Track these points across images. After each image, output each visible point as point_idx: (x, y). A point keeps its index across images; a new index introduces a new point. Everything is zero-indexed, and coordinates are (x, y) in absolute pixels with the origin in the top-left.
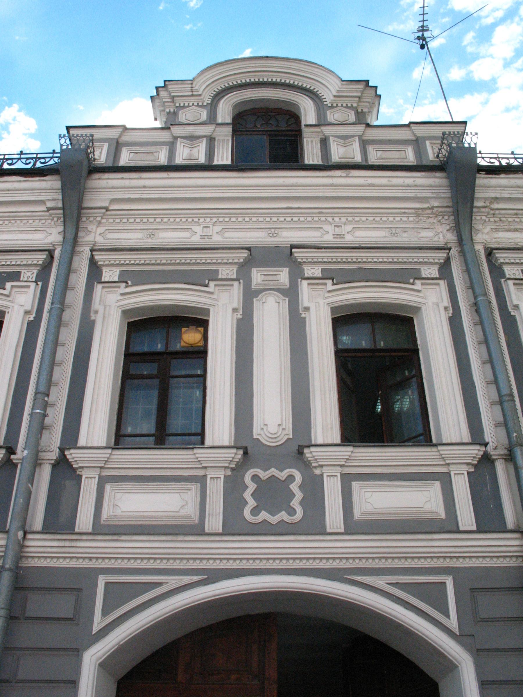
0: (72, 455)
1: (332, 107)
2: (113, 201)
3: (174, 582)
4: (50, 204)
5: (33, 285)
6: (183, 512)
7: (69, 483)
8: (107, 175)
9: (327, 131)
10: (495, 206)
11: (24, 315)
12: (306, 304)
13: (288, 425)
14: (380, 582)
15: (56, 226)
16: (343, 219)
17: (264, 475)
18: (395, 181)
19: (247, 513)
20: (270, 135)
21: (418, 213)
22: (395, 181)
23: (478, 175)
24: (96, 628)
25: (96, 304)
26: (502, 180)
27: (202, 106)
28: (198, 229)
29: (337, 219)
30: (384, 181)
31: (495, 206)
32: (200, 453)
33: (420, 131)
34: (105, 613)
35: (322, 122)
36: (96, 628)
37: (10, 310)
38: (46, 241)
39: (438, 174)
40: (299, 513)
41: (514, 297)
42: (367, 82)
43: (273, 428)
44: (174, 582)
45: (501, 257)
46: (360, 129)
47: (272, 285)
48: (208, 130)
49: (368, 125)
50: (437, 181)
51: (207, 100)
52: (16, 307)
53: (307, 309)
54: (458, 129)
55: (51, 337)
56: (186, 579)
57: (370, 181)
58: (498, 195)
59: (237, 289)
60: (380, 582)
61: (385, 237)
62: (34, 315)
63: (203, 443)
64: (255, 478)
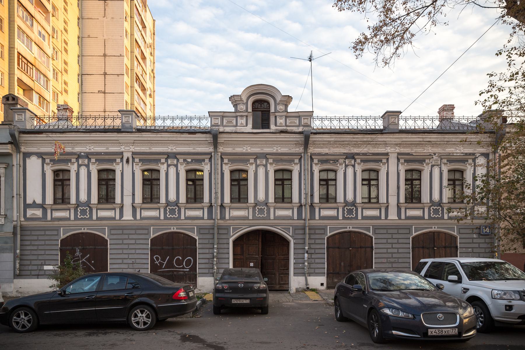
0: (224, 205)
1: (279, 104)
2: (225, 141)
3: (244, 227)
4: (209, 141)
6: (245, 215)
7: (223, 209)
8: (222, 134)
9: (277, 114)
10: (314, 142)
12: (269, 170)
13: (264, 198)
14: (279, 227)
15: (211, 146)
16: (278, 146)
17: (260, 208)
18: (291, 136)
19: (256, 215)
20: (262, 112)
21: (296, 144)
22: (291, 136)
23: (311, 135)
24: (231, 235)
25: (224, 169)
26: (317, 136)
27: (244, 104)
28: (244, 148)
29: (277, 146)
30: (288, 136)
31: (314, 142)
32: (248, 204)
33: (300, 114)
34: (232, 233)
35: (276, 111)
36: (231, 235)
38: (209, 151)
39: (302, 135)
40: (266, 215)
41: (314, 168)
42: (289, 96)
43: (261, 199)
44: (244, 227)
45: (313, 157)
46: (285, 114)
47: (261, 164)
48: (246, 114)
49: (288, 112)
50: (301, 136)
51: (245, 101)
52: (206, 169)
53: (269, 171)
54: (310, 114)
56: (246, 227)
57: (285, 136)
58: (316, 140)
59: (254, 165)
60: (279, 227)
61: (288, 150)
63: (248, 202)
64: (258, 208)
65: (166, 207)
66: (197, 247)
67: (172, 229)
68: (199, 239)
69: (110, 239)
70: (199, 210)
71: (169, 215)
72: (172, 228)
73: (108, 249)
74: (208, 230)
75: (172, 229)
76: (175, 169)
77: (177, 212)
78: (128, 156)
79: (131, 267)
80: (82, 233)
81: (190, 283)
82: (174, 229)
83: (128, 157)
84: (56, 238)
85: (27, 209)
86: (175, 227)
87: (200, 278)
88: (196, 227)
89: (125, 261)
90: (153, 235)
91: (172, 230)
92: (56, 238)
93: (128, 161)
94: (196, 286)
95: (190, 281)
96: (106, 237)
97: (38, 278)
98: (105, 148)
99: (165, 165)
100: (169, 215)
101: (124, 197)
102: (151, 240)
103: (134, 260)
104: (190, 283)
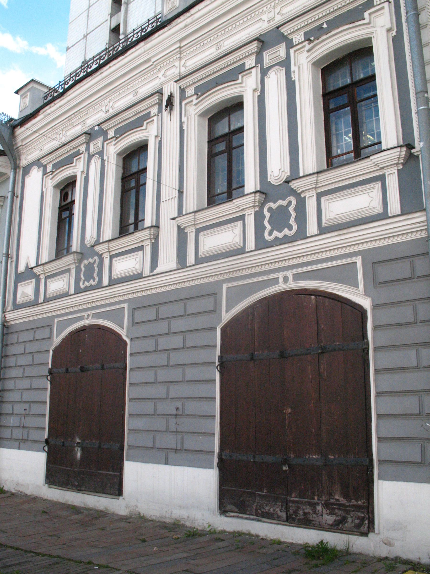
5: (386, 5)
11: (387, 34)
37: (374, 34)
52: (379, 29)
55: (415, 43)
62: (395, 30)
65: (262, 205)
66: (368, 344)
67: (281, 280)
68: (375, 307)
69: (132, 339)
70: (368, 186)
71: (270, 234)
72: (281, 275)
73: (125, 368)
74: (407, 264)
75: (281, 280)
76: (283, 71)
77: (293, 214)
78: (172, 91)
79: (173, 427)
80: (83, 329)
81: (343, 501)
82: (286, 279)
83: (171, 93)
84: (43, 346)
85: (19, 284)
86: (290, 274)
87: (380, 482)
88: (358, 260)
89: (162, 407)
90: (227, 311)
91: (281, 287)
92: (43, 346)
93: (170, 103)
94: (371, 522)
95: (346, 496)
96: (123, 333)
97: (19, 448)
98: (131, 96)
99: (255, 74)
100: (270, 234)
101: (162, 205)
102: (223, 330)
103: (179, 404)
104: (343, 501)
